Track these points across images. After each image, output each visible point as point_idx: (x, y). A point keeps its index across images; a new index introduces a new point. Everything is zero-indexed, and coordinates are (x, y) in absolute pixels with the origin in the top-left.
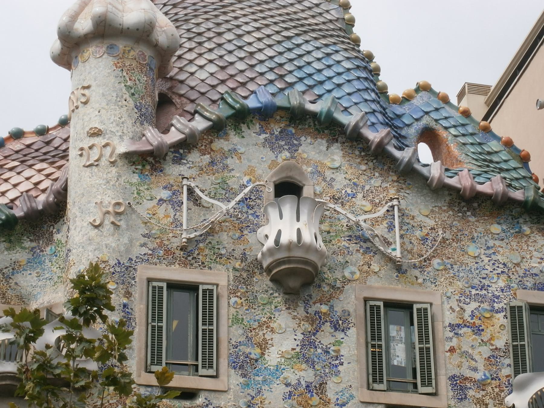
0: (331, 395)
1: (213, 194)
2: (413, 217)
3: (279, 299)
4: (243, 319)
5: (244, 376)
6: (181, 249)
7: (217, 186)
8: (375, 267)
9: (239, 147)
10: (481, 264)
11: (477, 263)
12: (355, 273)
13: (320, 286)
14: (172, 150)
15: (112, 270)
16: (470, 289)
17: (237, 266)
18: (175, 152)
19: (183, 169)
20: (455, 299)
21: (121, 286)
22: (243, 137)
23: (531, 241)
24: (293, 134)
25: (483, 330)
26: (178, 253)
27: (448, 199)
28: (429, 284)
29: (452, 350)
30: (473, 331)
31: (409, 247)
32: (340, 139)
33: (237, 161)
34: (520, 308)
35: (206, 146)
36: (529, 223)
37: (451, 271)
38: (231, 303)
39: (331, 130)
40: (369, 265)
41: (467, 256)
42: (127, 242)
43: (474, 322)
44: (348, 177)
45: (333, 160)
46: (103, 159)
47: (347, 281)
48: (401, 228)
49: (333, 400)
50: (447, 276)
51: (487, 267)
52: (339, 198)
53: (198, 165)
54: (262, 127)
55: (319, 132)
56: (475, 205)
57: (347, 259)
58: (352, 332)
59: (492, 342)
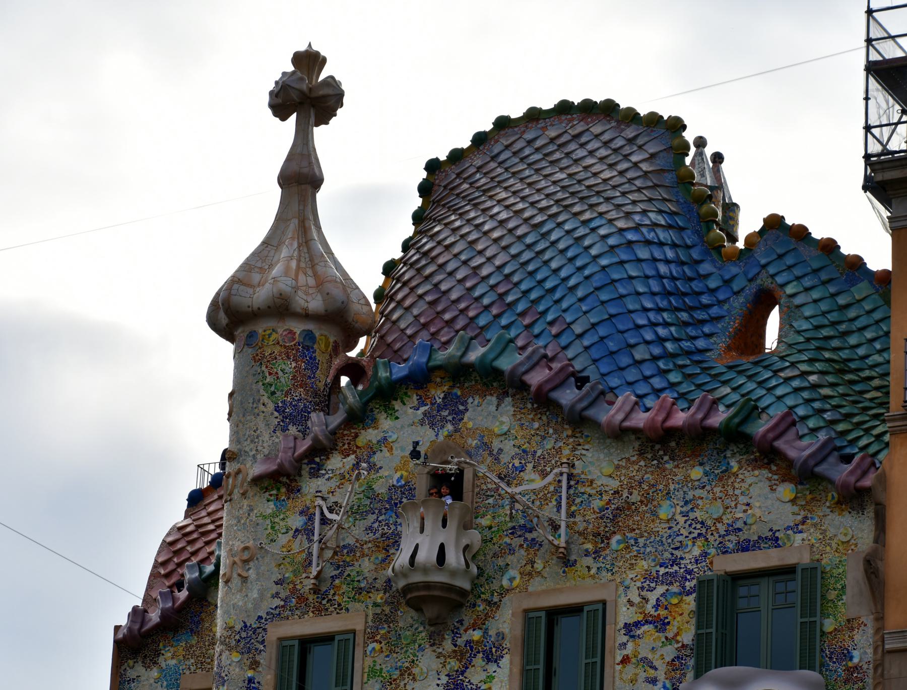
1: (356, 507)
2: (592, 482)
3: (423, 634)
4: (381, 669)
6: (314, 593)
7: (361, 496)
8: (539, 566)
9: (390, 434)
10: (675, 529)
11: (670, 528)
12: (514, 578)
13: (474, 605)
14: (306, 461)
15: (237, 637)
16: (658, 568)
17: (379, 601)
18: (312, 462)
19: (320, 484)
20: (635, 588)
21: (246, 656)
22: (397, 418)
23: (738, 480)
24: (458, 397)
25: (669, 623)
27: (637, 444)
28: (604, 573)
29: (625, 660)
30: (656, 627)
31: (581, 527)
32: (510, 391)
33: (388, 454)
34: (710, 581)
35: (349, 444)
36: (737, 455)
37: (635, 548)
38: (368, 653)
39: (499, 381)
40: (533, 563)
41: (658, 521)
42: (255, 596)
43: (659, 615)
44: (517, 442)
45: (502, 423)
46: (236, 491)
48: (569, 505)
50: (628, 556)
51: (685, 532)
52: (505, 476)
53: (338, 472)
54: (421, 398)
55: (488, 386)
56: (673, 444)
57: (508, 561)
58: (505, 661)
59: (679, 638)
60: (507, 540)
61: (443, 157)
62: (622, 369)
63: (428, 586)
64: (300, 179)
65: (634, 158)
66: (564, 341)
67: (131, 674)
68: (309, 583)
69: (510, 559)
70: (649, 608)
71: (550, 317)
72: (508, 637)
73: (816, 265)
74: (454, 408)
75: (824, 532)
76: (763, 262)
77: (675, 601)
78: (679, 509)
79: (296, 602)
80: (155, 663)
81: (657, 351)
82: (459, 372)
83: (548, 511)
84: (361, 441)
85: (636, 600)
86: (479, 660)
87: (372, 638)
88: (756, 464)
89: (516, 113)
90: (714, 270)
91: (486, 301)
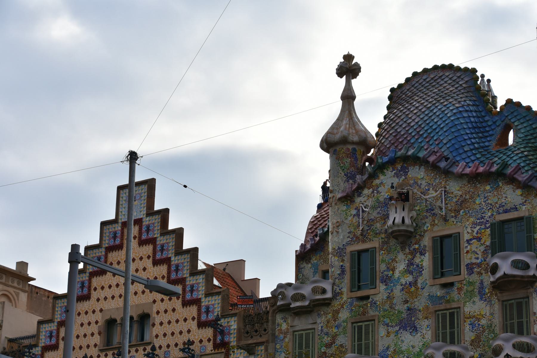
0: (419, 285)
5: (386, 285)
8: (436, 222)
19: (361, 198)
26: (360, 237)
27: (467, 179)
29: (468, 252)
31: (450, 208)
34: (495, 224)
44: (426, 181)
47: (425, 231)
48: (445, 201)
49: (420, 287)
56: (479, 178)
60: (425, 214)
61: (396, 87)
62: (461, 154)
63: (399, 231)
64: (348, 97)
65: (460, 83)
66: (440, 146)
67: (302, 266)
68: (359, 232)
69: (426, 220)
70: (475, 234)
71: (435, 138)
72: (427, 247)
73: (524, 115)
74: (404, 171)
75: (532, 205)
76: (506, 115)
77: (483, 231)
78: (483, 200)
79: (355, 239)
80: (310, 262)
81: (472, 147)
82: (405, 159)
83: (438, 203)
84: (374, 184)
85: (470, 231)
86: (418, 255)
87: (382, 249)
88: (508, 183)
89: (419, 70)
90: (489, 119)
91: (413, 134)
